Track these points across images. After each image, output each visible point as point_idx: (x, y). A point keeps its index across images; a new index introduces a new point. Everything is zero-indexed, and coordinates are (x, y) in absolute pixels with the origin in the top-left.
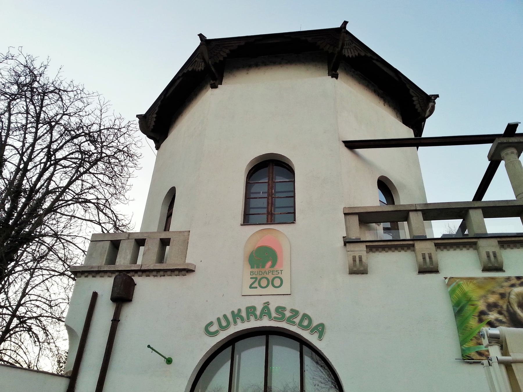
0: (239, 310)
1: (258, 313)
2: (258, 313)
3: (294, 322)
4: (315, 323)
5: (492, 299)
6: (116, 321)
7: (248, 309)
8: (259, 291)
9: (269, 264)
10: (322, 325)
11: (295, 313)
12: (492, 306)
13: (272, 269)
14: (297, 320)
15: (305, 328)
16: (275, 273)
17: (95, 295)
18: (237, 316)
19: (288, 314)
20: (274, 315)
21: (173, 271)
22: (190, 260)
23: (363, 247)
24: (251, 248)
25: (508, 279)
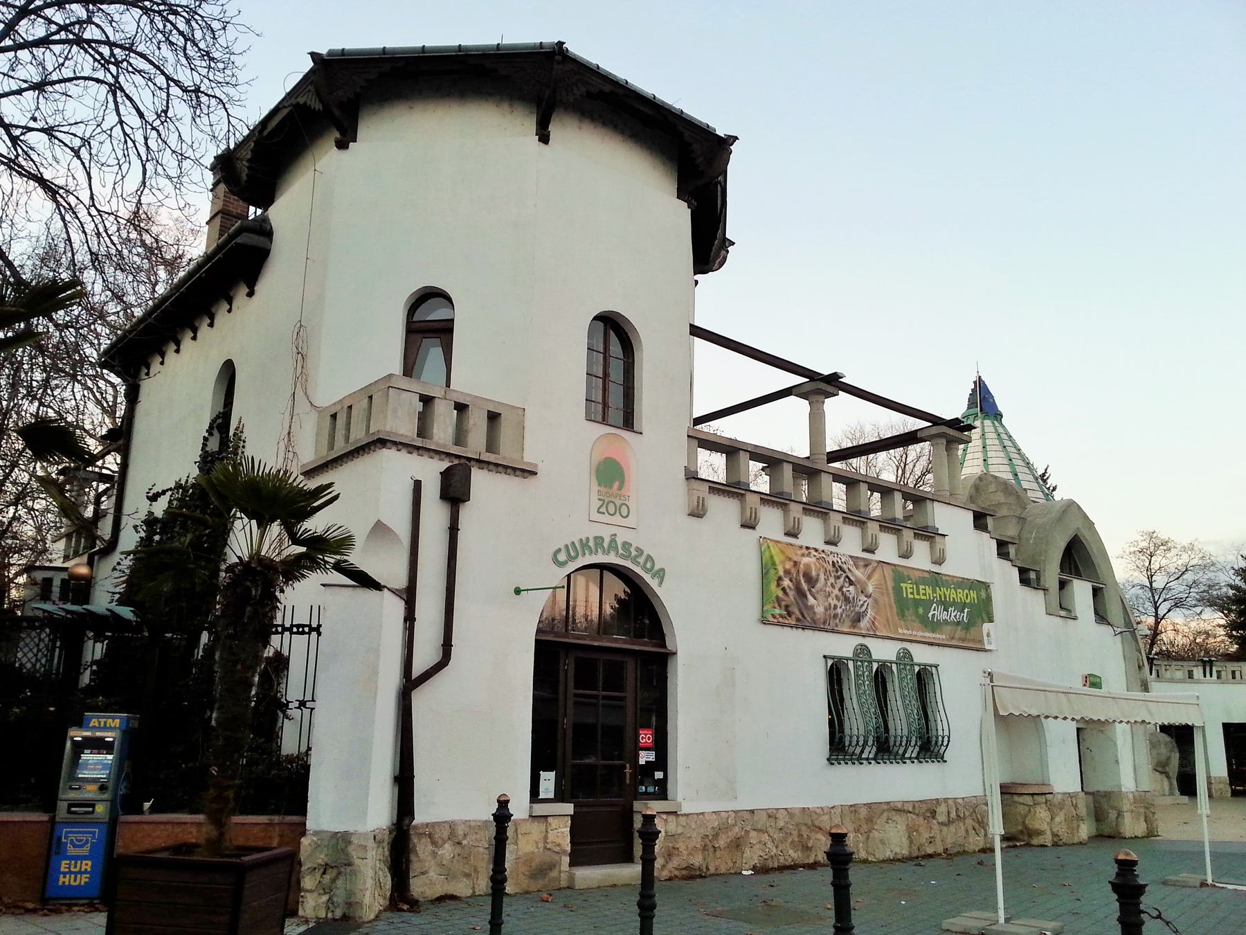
0: (588, 539)
1: (606, 545)
2: (606, 545)
3: (639, 563)
4: (657, 568)
5: (788, 565)
6: (453, 530)
7: (596, 538)
8: (605, 518)
9: (616, 484)
10: (663, 570)
11: (640, 551)
12: (787, 572)
13: (620, 493)
14: (641, 560)
15: (647, 571)
16: (622, 498)
17: (417, 485)
18: (584, 544)
19: (634, 553)
20: (621, 551)
21: (506, 467)
22: (530, 457)
23: (706, 487)
24: (597, 458)
25: (801, 547)
